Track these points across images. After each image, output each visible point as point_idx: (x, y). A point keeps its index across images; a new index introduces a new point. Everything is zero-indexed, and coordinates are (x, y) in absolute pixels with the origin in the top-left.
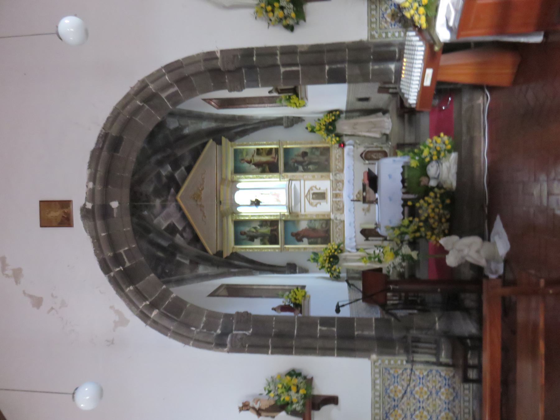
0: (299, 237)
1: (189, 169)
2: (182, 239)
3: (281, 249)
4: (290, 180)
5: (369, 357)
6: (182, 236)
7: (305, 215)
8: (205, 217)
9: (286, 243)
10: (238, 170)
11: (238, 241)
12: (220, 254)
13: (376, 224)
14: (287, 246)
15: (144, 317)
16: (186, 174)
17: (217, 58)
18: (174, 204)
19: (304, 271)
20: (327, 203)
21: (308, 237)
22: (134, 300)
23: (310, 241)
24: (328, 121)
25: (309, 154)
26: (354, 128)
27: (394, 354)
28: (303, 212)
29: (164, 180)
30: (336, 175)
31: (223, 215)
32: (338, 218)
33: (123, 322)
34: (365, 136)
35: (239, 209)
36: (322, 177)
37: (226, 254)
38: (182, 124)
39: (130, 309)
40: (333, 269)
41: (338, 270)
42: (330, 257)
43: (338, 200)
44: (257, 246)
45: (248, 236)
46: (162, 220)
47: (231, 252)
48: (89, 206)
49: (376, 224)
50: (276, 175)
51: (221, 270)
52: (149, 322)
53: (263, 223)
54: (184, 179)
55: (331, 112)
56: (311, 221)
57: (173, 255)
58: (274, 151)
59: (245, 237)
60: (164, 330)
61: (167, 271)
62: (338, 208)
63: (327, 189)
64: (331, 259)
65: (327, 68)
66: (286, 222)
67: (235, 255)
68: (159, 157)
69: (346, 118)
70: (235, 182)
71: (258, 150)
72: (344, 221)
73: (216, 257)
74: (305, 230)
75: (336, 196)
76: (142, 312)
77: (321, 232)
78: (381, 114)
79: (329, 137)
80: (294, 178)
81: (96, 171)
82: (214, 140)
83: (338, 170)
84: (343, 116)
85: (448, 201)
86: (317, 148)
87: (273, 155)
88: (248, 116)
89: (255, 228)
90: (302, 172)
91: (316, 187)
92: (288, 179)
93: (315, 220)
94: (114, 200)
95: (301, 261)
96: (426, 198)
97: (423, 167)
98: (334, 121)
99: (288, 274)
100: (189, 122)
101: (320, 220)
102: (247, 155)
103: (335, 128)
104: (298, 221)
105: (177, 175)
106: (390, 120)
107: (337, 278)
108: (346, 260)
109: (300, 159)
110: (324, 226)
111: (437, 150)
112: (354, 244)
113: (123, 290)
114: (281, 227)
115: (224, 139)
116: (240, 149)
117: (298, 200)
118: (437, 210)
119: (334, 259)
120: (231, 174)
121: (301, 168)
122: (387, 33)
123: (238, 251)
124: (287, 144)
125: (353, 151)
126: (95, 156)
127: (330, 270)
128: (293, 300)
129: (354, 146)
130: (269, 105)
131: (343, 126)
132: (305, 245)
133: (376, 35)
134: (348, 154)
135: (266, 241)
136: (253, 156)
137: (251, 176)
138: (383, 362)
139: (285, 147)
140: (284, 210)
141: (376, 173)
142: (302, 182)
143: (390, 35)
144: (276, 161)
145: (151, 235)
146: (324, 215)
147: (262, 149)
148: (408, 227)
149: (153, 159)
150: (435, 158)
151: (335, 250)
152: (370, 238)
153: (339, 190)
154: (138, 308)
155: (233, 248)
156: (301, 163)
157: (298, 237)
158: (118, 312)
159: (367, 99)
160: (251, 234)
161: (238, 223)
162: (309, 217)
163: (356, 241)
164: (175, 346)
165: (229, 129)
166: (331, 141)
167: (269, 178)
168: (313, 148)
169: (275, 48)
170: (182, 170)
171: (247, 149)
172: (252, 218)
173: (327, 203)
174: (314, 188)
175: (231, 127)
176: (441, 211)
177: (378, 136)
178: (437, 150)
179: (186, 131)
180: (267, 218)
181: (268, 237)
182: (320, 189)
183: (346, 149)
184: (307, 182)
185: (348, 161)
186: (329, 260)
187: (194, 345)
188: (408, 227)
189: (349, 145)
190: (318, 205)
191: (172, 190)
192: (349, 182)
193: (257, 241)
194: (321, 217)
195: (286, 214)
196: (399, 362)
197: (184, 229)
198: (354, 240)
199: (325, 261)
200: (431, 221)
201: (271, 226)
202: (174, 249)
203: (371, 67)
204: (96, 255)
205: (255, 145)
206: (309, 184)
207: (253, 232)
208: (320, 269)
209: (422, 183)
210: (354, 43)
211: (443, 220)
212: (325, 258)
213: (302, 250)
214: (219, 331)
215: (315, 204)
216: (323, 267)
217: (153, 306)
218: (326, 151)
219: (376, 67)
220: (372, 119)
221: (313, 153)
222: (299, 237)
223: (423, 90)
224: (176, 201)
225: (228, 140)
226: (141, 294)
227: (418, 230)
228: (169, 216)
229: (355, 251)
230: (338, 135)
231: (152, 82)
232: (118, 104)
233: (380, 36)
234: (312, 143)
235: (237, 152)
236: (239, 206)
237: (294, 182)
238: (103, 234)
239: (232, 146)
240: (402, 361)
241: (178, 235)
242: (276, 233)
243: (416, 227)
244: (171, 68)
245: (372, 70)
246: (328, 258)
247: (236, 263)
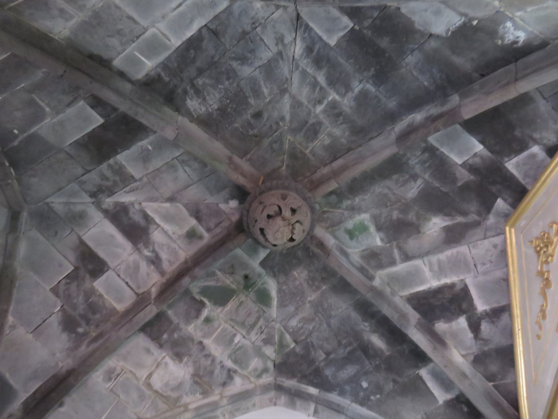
2: (471, 335)
6: (475, 327)
8: (544, 317)
46: (426, 270)
61: (365, 385)
105: (512, 165)
170: (533, 156)
241: (462, 322)
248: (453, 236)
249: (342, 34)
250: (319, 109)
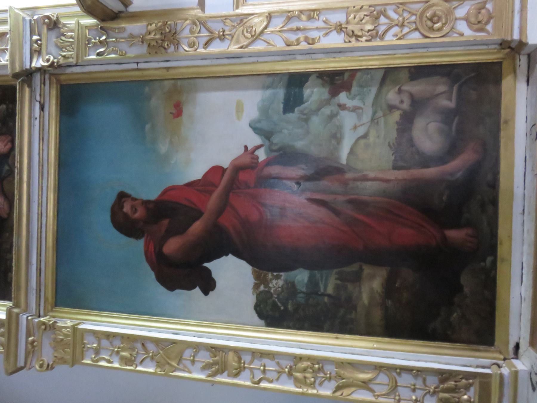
0: (172, 246)
9: (68, 293)
14: (67, 320)
21: (263, 257)
23: (277, 283)
56: (296, 82)
66: (75, 96)
93: (336, 81)
101: (389, 74)
110: (428, 136)
222: (172, 246)
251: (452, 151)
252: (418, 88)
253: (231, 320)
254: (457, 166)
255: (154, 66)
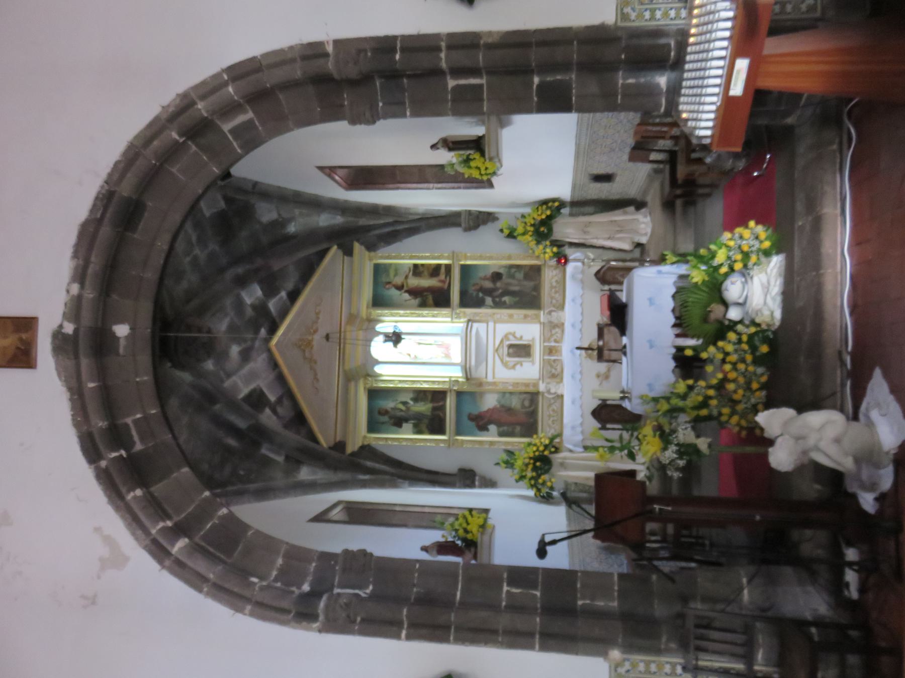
0: (481, 423)
1: (293, 296)
2: (274, 418)
3: (449, 443)
4: (469, 321)
5: (604, 654)
6: (274, 411)
7: (494, 384)
8: (318, 380)
9: (458, 433)
10: (379, 302)
11: (373, 427)
12: (340, 446)
13: (623, 392)
15: (159, 551)
16: (288, 303)
17: (326, 55)
18: (264, 356)
19: (490, 483)
20: (533, 362)
21: (499, 424)
22: (143, 518)
23: (501, 429)
24: (539, 218)
25: (504, 277)
26: (585, 233)
27: (658, 652)
28: (490, 379)
29: (249, 312)
30: (550, 313)
31: (350, 377)
32: (553, 391)
33: (117, 560)
34: (603, 248)
35: (378, 369)
36: (526, 316)
37: (350, 449)
38: (285, 215)
39: (133, 534)
40: (540, 481)
41: (549, 484)
42: (536, 459)
43: (553, 358)
44: (406, 434)
45: (391, 418)
47: (360, 444)
48: (69, 328)
49: (623, 392)
50: (445, 311)
51: (340, 476)
52: (167, 563)
53: (420, 395)
54: (284, 313)
55: (545, 202)
56: (504, 393)
57: (257, 444)
58: (443, 270)
59: (385, 419)
60: (196, 580)
61: (242, 473)
62: (554, 373)
63: (533, 339)
64: (538, 464)
65: (536, 80)
66: (459, 394)
67: (367, 451)
68: (240, 270)
69: (571, 215)
70: (372, 322)
71: (416, 266)
72: (562, 396)
73: (333, 453)
74: (492, 411)
75: (551, 351)
76: (155, 541)
77: (521, 414)
78: (631, 209)
79: (541, 247)
80: (477, 318)
81: (87, 263)
82: (340, 246)
83: (554, 306)
84: (565, 211)
85: (764, 349)
86: (518, 267)
87: (442, 277)
88: (400, 208)
89: (405, 403)
90: (492, 307)
91: (514, 335)
92: (466, 319)
93: (511, 393)
94: (121, 322)
95: (484, 465)
96: (720, 344)
97: (715, 289)
98: (550, 218)
99: (460, 487)
100: (297, 212)
101: (521, 393)
102: (396, 275)
103: (550, 230)
104: (482, 394)
106: (649, 218)
107: (547, 499)
108: (563, 465)
109: (488, 284)
110: (527, 403)
111: (742, 252)
112: (580, 437)
113: (121, 497)
114: (450, 403)
115: (357, 247)
116: (385, 265)
117: (482, 357)
118: (741, 367)
119: (542, 463)
120: (367, 307)
121: (489, 300)
122: (653, 11)
123: (374, 443)
124: (466, 258)
125: (583, 272)
126: (88, 234)
127: (535, 484)
128: (461, 532)
129: (583, 263)
130: (436, 185)
131: (567, 228)
132: (491, 436)
133: (633, 16)
134: (573, 277)
135: (424, 427)
136: (407, 277)
137: (402, 312)
138: (634, 666)
139: (462, 263)
140: (457, 373)
141: (624, 300)
142: (491, 324)
143: (658, 14)
144: (446, 286)
145: (217, 407)
146: (527, 385)
147: (423, 265)
148: (684, 397)
149: (230, 274)
150: (738, 266)
151: (546, 447)
152: (609, 426)
153: (556, 341)
154: (146, 532)
155: (365, 437)
156: (489, 292)
157: (481, 422)
158: (108, 540)
159: (606, 178)
160: (399, 414)
161: (374, 394)
162: (500, 387)
163: (582, 432)
164: (217, 612)
165: (368, 229)
166: (545, 253)
167: (433, 316)
168: (511, 267)
169: (437, 36)
170: (282, 298)
171: (396, 264)
172: (400, 386)
173: (533, 362)
174: (511, 337)
175: (369, 226)
176: (751, 368)
177: (626, 246)
178: (742, 252)
179: (292, 229)
180: (425, 386)
181: (426, 421)
182: (521, 337)
183: (570, 268)
184: (499, 326)
185: (572, 289)
186: (534, 464)
187: (252, 615)
188: (684, 397)
189: (576, 260)
190: (518, 367)
191: (263, 332)
192: (573, 326)
193: (408, 426)
194: (523, 389)
195: (460, 380)
196: (667, 669)
197: (279, 401)
198: (579, 429)
199: (527, 465)
200: (731, 387)
201: (432, 401)
202: (257, 435)
203: (621, 82)
204: (76, 425)
205: (411, 258)
206: (503, 329)
207: (401, 410)
208: (517, 481)
209: (713, 316)
210: (589, 28)
211: (755, 386)
212: (527, 461)
213: (487, 446)
214: (306, 588)
215: (511, 364)
216: (522, 477)
217: (179, 530)
218: (534, 272)
219: (631, 81)
220: (617, 216)
221: (512, 276)
223: (729, 104)
224: (269, 351)
225: (363, 248)
226: (157, 507)
227: (704, 404)
228: (253, 375)
229: (581, 450)
230: (555, 243)
231: (203, 97)
232: (137, 137)
233: (640, 16)
234: (509, 258)
235: (378, 270)
236: (377, 362)
237: (475, 325)
238: (91, 385)
239: (371, 260)
240: (673, 666)
241: (268, 411)
242: (441, 414)
243: (700, 398)
244: (240, 72)
245: (622, 84)
246: (532, 461)
247: (369, 464)
248: (246, 356)
249: (215, 210)
250: (188, 259)
251: (530, 406)
252: (525, 395)
253: (493, 436)
254: (532, 408)
255: (477, 389)
